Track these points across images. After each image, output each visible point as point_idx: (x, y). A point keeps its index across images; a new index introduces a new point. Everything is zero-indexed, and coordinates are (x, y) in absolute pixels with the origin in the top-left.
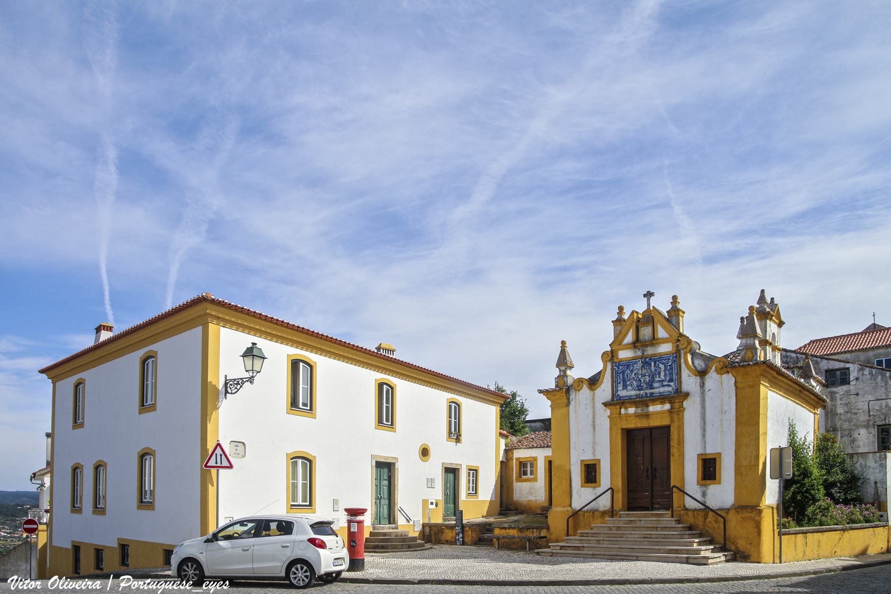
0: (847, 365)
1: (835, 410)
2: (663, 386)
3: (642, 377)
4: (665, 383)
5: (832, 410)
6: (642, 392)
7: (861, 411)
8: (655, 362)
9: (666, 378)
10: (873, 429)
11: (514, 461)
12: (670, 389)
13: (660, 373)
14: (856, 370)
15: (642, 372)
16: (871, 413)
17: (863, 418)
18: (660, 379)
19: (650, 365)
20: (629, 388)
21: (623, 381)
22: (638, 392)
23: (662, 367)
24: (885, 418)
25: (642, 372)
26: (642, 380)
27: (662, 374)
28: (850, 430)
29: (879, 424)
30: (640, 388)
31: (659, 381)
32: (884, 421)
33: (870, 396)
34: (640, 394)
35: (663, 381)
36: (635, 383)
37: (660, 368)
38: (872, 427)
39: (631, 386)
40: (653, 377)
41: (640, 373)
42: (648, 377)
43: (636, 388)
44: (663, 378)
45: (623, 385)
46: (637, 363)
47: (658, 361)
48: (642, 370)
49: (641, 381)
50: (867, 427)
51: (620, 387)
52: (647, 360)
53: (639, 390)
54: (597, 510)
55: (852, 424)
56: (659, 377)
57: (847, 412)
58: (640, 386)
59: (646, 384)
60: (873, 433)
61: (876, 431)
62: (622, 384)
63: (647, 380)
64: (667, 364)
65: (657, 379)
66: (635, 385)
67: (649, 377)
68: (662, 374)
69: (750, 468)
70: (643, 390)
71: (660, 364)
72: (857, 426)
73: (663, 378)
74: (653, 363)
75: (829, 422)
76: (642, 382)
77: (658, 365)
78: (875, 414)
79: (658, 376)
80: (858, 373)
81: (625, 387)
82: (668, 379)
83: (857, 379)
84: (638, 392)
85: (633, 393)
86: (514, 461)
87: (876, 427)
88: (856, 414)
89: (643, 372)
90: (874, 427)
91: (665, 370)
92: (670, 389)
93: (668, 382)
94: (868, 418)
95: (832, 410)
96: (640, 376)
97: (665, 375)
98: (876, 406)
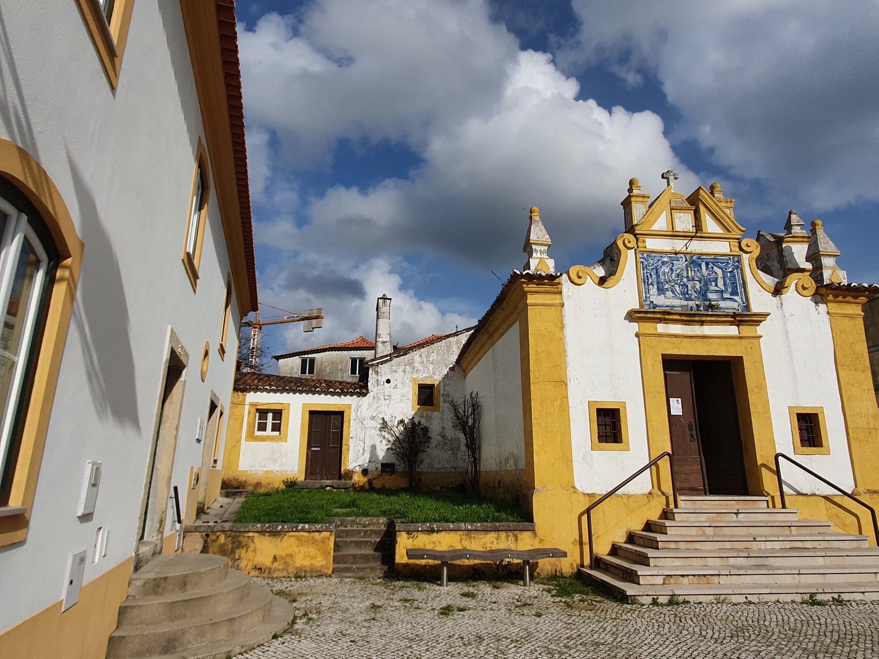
2: (724, 299)
3: (688, 280)
4: (725, 296)
6: (691, 303)
8: (707, 264)
9: (726, 290)
11: (247, 407)
12: (735, 305)
13: (716, 280)
15: (687, 273)
18: (717, 289)
19: (700, 265)
20: (669, 294)
21: (658, 283)
22: (685, 303)
23: (719, 272)
25: (687, 273)
26: (689, 286)
27: (720, 282)
30: (686, 296)
31: (717, 291)
34: (687, 305)
35: (722, 292)
36: (678, 288)
37: (715, 273)
39: (673, 292)
40: (706, 284)
41: (685, 275)
42: (698, 282)
43: (681, 296)
44: (723, 288)
45: (658, 288)
46: (679, 260)
47: (712, 263)
48: (687, 270)
49: (687, 286)
51: (654, 290)
52: (694, 258)
53: (687, 299)
54: (629, 496)
56: (716, 286)
58: (687, 293)
59: (695, 292)
62: (656, 286)
63: (698, 287)
64: (726, 269)
65: (713, 287)
66: (679, 292)
67: (700, 283)
68: (720, 282)
69: (870, 433)
70: (692, 300)
71: (714, 267)
73: (723, 288)
74: (703, 265)
76: (690, 288)
77: (713, 268)
79: (713, 284)
81: (661, 291)
82: (730, 290)
84: (685, 303)
85: (677, 302)
86: (247, 407)
89: (690, 275)
91: (724, 278)
92: (735, 305)
93: (731, 294)
96: (685, 280)
97: (725, 284)
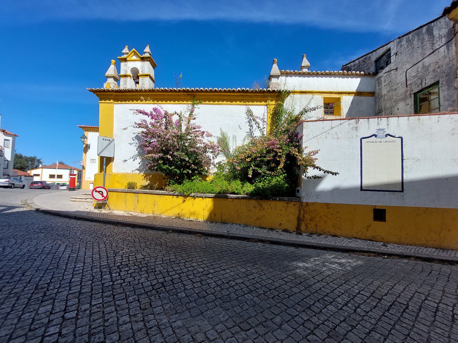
0: (388, 46)
1: (381, 93)
5: (379, 94)
7: (399, 85)
10: (410, 99)
14: (395, 46)
16: (408, 83)
17: (402, 90)
24: (422, 81)
28: (391, 108)
29: (416, 91)
32: (420, 86)
33: (407, 66)
38: (409, 97)
50: (404, 99)
55: (393, 101)
57: (389, 92)
60: (410, 104)
61: (413, 100)
72: (396, 102)
75: (377, 106)
78: (411, 81)
80: (397, 48)
83: (396, 54)
87: (413, 96)
88: (396, 89)
90: (411, 97)
94: (405, 89)
95: (379, 94)
98: (412, 73)
